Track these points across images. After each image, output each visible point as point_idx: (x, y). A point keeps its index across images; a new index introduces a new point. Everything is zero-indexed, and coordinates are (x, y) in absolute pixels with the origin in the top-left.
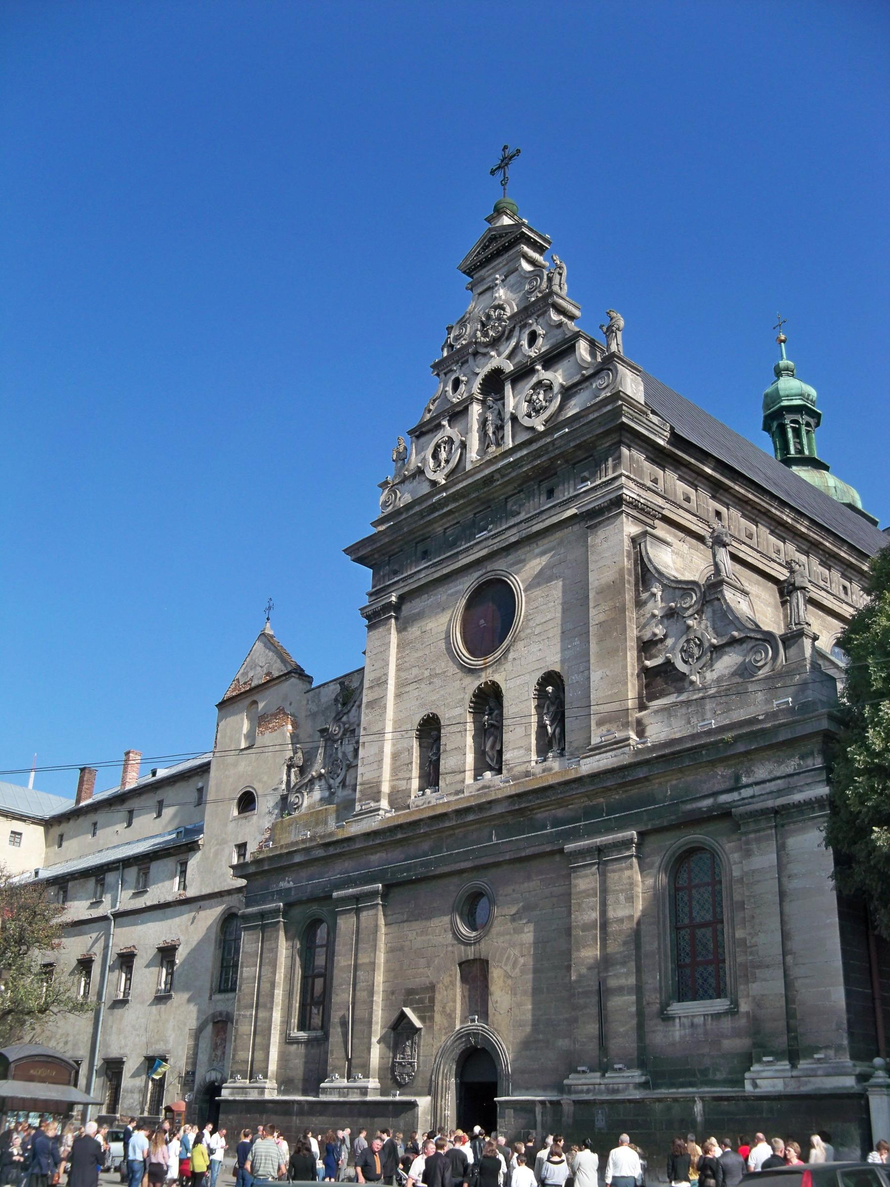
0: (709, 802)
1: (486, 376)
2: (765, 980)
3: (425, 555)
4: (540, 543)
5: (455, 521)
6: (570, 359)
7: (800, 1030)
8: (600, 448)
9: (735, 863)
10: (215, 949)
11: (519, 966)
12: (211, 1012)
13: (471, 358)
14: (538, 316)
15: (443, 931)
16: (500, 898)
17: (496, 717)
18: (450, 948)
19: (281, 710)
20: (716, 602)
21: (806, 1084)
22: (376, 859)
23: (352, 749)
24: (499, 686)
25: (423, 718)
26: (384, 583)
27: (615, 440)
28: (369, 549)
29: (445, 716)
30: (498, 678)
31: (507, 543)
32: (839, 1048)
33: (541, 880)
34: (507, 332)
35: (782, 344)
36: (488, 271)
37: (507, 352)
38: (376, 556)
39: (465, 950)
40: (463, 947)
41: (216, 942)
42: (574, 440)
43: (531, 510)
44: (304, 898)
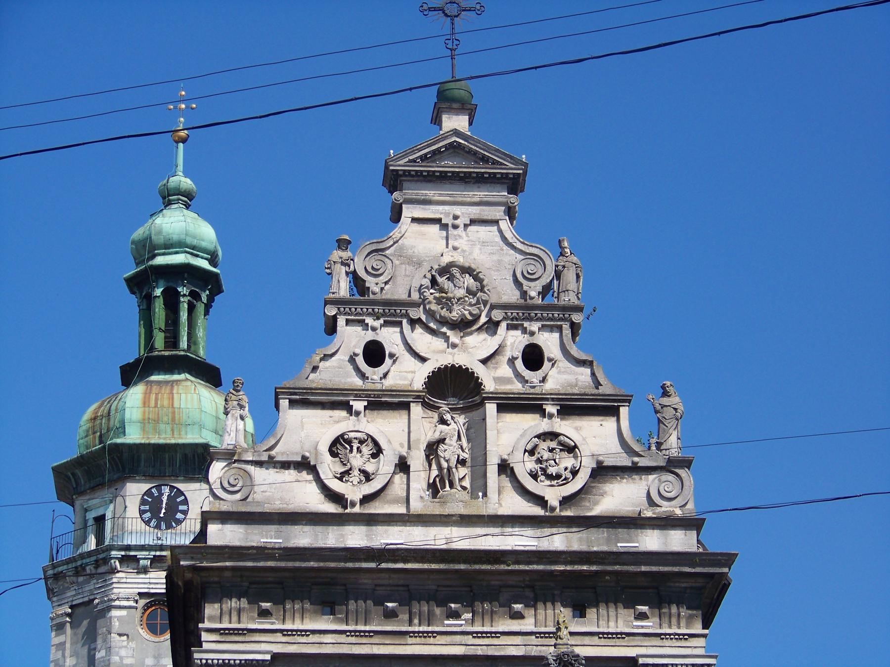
1: (439, 368)
5: (401, 582)
6: (603, 423)
8: (672, 584)
13: (405, 321)
27: (698, 585)
31: (502, 653)
34: (483, 319)
35: (181, 145)
36: (441, 195)
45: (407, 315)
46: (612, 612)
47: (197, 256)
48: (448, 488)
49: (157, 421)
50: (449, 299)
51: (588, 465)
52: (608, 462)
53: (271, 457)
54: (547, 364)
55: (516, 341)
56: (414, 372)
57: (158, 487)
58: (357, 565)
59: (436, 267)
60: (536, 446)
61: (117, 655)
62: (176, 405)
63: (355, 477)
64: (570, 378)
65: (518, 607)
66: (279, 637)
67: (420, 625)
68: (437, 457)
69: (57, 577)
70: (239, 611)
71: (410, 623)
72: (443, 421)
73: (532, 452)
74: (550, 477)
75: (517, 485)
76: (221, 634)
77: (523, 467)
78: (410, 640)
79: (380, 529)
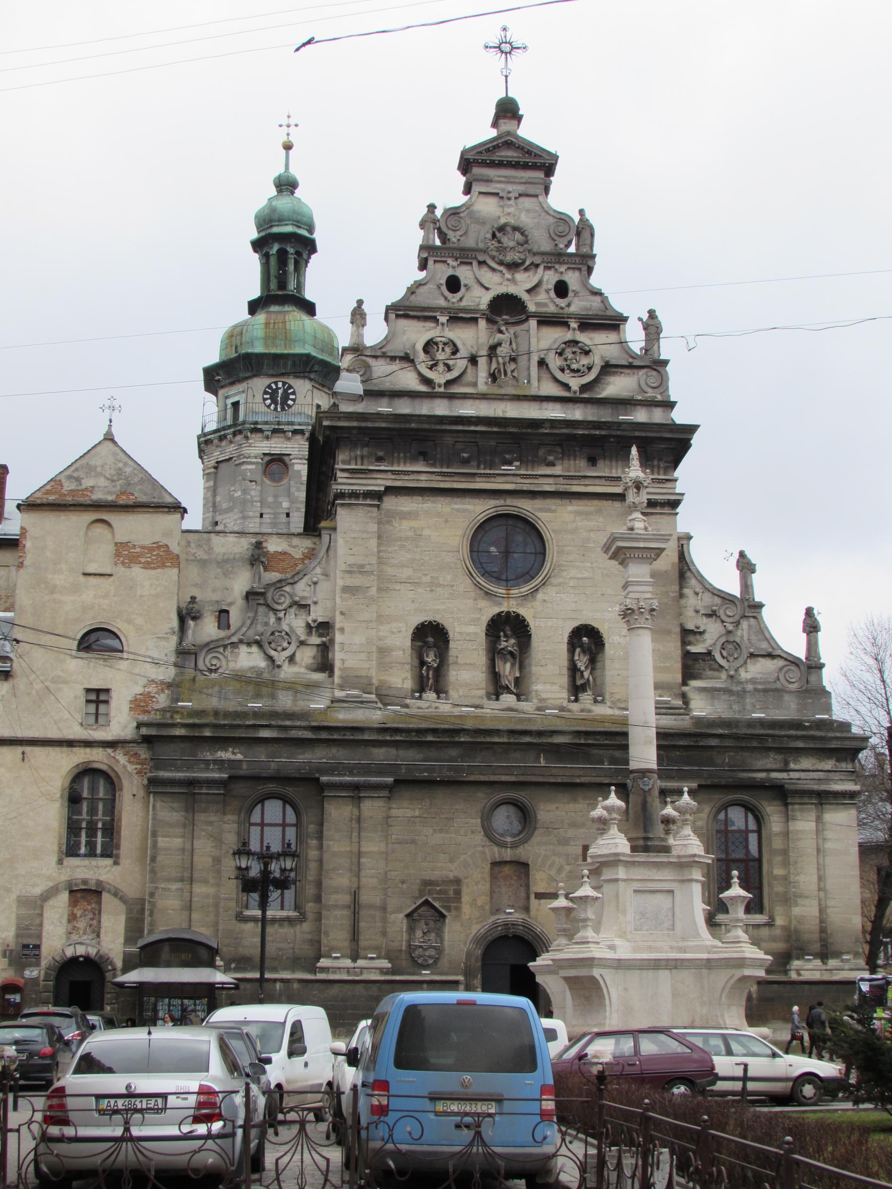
0: (762, 775)
2: (804, 906)
3: (424, 455)
4: (574, 501)
7: (830, 941)
9: (775, 822)
10: (62, 805)
11: (565, 873)
12: (64, 876)
13: (475, 263)
14: (569, 268)
15: (469, 832)
16: (541, 813)
17: (513, 647)
18: (480, 848)
19: (159, 547)
20: (752, 619)
21: (836, 974)
22: (380, 755)
23: (304, 625)
24: (525, 620)
25: (422, 624)
26: (362, 464)
28: (355, 424)
29: (455, 630)
30: (525, 612)
31: (540, 489)
32: (856, 954)
33: (589, 805)
34: (528, 263)
36: (499, 176)
37: (529, 286)
38: (354, 432)
39: (499, 852)
40: (496, 849)
41: (62, 796)
42: (640, 431)
43: (572, 469)
44: (264, 775)
45: (476, 258)
46: (614, 463)
47: (300, 227)
48: (503, 377)
49: (275, 338)
50: (505, 248)
51: (598, 363)
52: (611, 363)
53: (384, 353)
54: (571, 294)
55: (550, 278)
56: (480, 297)
57: (276, 383)
58: (444, 427)
59: (496, 226)
60: (563, 350)
61: (249, 494)
62: (288, 327)
63: (441, 367)
64: (587, 304)
65: (551, 458)
66: (390, 476)
67: (484, 469)
68: (496, 356)
69: (208, 442)
70: (362, 458)
71: (478, 467)
72: (501, 332)
73: (560, 354)
74: (573, 371)
75: (549, 376)
76: (351, 473)
77: (554, 362)
78: (478, 479)
79: (457, 403)
